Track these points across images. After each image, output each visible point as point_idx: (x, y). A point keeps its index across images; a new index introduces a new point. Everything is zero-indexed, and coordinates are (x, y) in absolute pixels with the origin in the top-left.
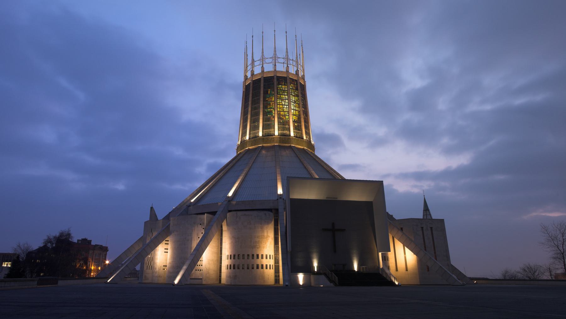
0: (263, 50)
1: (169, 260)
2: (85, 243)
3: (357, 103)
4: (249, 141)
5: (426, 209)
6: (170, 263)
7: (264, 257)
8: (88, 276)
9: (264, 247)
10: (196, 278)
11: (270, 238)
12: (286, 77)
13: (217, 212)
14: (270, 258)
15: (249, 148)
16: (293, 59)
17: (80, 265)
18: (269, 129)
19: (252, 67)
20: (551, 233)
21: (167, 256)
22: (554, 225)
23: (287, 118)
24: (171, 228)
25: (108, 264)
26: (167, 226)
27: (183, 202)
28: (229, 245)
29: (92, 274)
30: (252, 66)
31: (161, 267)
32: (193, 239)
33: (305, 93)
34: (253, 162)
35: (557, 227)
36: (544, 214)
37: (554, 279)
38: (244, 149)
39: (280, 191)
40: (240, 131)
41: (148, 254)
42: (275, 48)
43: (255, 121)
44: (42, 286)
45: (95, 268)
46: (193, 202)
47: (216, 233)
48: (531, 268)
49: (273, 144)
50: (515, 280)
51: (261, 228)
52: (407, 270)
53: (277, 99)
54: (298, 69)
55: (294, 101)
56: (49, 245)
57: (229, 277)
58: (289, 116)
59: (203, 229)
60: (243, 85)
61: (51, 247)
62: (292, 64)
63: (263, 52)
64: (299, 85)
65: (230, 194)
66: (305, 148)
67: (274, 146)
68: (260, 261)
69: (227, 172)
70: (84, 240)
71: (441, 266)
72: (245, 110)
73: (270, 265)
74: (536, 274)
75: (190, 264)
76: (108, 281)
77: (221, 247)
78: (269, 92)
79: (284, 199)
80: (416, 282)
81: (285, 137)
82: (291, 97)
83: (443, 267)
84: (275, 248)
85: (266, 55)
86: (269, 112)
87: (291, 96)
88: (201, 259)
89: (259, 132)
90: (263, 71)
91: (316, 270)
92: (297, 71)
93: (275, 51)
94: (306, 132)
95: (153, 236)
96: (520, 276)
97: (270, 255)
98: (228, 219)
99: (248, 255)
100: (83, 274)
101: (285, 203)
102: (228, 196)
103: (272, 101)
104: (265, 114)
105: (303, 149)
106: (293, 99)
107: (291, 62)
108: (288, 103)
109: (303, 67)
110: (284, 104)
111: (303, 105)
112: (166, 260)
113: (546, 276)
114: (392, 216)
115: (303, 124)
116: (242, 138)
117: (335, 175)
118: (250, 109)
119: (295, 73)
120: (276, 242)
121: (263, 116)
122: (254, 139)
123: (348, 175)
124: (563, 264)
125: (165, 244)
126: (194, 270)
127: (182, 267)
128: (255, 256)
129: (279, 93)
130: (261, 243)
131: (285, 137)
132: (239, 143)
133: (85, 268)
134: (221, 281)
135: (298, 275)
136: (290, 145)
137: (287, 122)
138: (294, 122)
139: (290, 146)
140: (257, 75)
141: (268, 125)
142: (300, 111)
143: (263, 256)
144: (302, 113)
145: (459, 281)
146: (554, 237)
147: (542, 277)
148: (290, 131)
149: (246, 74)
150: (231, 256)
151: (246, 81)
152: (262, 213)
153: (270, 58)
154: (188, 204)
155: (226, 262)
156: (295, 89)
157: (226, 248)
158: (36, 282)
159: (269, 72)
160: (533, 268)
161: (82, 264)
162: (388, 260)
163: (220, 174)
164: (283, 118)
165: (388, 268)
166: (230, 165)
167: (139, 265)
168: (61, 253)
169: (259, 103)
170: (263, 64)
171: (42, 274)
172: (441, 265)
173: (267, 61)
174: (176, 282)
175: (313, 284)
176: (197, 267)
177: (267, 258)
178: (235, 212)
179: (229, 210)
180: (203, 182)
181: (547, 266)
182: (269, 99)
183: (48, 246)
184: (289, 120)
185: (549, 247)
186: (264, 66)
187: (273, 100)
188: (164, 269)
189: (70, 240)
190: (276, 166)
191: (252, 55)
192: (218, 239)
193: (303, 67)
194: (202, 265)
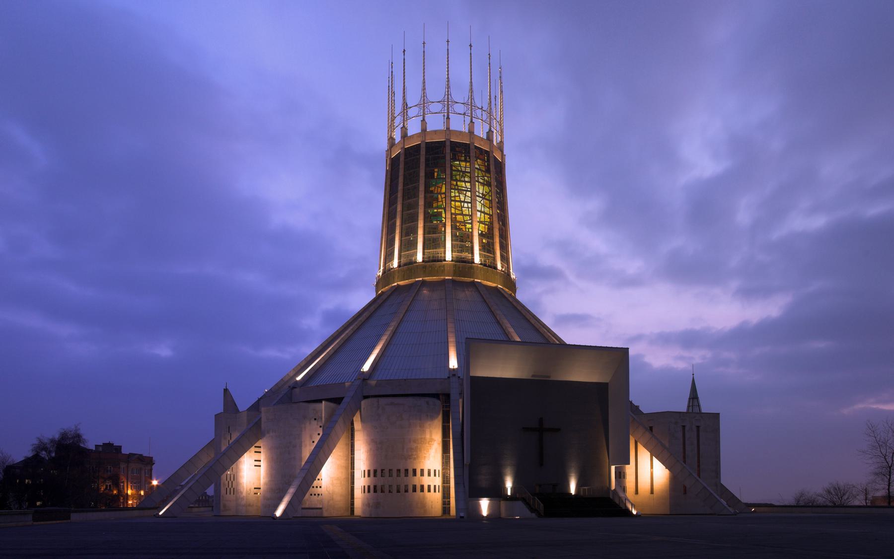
0: (424, 83)
1: (264, 479)
2: (110, 451)
3: (595, 204)
4: (399, 271)
5: (694, 397)
6: (265, 484)
7: (426, 473)
8: (123, 504)
9: (425, 457)
10: (313, 506)
11: (435, 442)
12: (469, 144)
13: (344, 398)
14: (435, 475)
15: (398, 283)
16: (482, 107)
17: (106, 488)
18: (436, 248)
19: (404, 120)
20: (879, 437)
21: (260, 472)
22: (887, 423)
23: (469, 229)
24: (263, 426)
25: (157, 485)
26: (256, 423)
27: (282, 379)
28: (366, 454)
29: (130, 502)
30: (404, 117)
31: (250, 490)
32: (303, 444)
33: (502, 179)
34: (407, 310)
35: (890, 427)
36: (875, 406)
37: (869, 504)
38: (390, 286)
39: (453, 363)
40: (381, 251)
41: (226, 469)
42: (448, 81)
43: (409, 232)
44: (42, 523)
45: (134, 492)
46: (299, 381)
47: (343, 433)
48: (839, 489)
49: (442, 277)
50: (812, 506)
51: (420, 426)
52: (652, 492)
53: (451, 189)
54: (492, 129)
55: (482, 194)
56: (43, 454)
57: (367, 505)
58: (471, 223)
59: (321, 427)
60: (387, 157)
61: (47, 459)
62: (480, 117)
63: (424, 89)
64: (492, 161)
65: (366, 367)
66: (499, 286)
67: (445, 280)
68: (419, 479)
69: (359, 328)
70: (108, 446)
71: (705, 487)
72: (391, 208)
73: (435, 486)
74: (845, 497)
75: (300, 485)
76: (161, 513)
77: (351, 457)
78: (436, 174)
79: (459, 377)
80: (664, 510)
81: (463, 264)
82: (477, 186)
83: (707, 487)
84: (443, 458)
85: (431, 96)
86: (435, 216)
87: (477, 183)
88: (318, 477)
89: (416, 253)
90: (424, 130)
91: (509, 493)
92: (490, 132)
93: (448, 87)
94: (502, 256)
95: (233, 439)
96: (821, 501)
97: (435, 471)
98: (362, 409)
99: (399, 471)
100: (115, 502)
101: (462, 385)
102: (362, 370)
103: (441, 194)
104: (428, 218)
105: (496, 288)
106: (481, 191)
107: (479, 112)
108: (471, 197)
109: (501, 125)
110: (463, 199)
111: (498, 203)
112: (259, 479)
113: (859, 501)
114: (637, 407)
115: (497, 240)
116: (385, 263)
117: (549, 336)
118: (398, 223)
119: (485, 137)
120: (445, 450)
121: (424, 223)
122: (408, 266)
123: (571, 336)
124: (887, 483)
125: (255, 452)
126: (307, 495)
127: (288, 490)
128: (411, 472)
129: (453, 178)
130: (421, 451)
131: (463, 264)
132: (381, 274)
133: (115, 492)
134: (354, 511)
135: (480, 501)
136: (472, 279)
137: (468, 235)
138: (481, 235)
139: (473, 282)
140: (412, 136)
141: (434, 241)
142: (492, 215)
143: (423, 471)
144: (495, 218)
145: (728, 507)
146: (882, 442)
147: (853, 502)
148: (472, 253)
149: (391, 134)
150: (369, 471)
151: (392, 148)
152: (422, 401)
153: (439, 102)
154: (291, 383)
155: (360, 482)
156: (484, 170)
157: (360, 460)
158: (30, 517)
159: (435, 132)
160: (842, 488)
161: (110, 486)
162: (624, 478)
163: (347, 332)
164: (461, 227)
165: (624, 489)
166: (365, 315)
167: (213, 485)
168: (68, 468)
169: (416, 196)
170: (424, 114)
171: (38, 503)
172: (705, 485)
174: (278, 513)
175: (503, 515)
176: (311, 490)
177: (429, 475)
178: (375, 399)
179: (365, 395)
180: (315, 346)
181: (863, 486)
182: (436, 190)
183: (42, 456)
184: (472, 232)
185: (871, 458)
186: (426, 119)
187: (443, 190)
188: (257, 494)
189: (82, 445)
190: (447, 319)
191: (404, 93)
192: (347, 444)
193: (501, 125)
194: (320, 487)
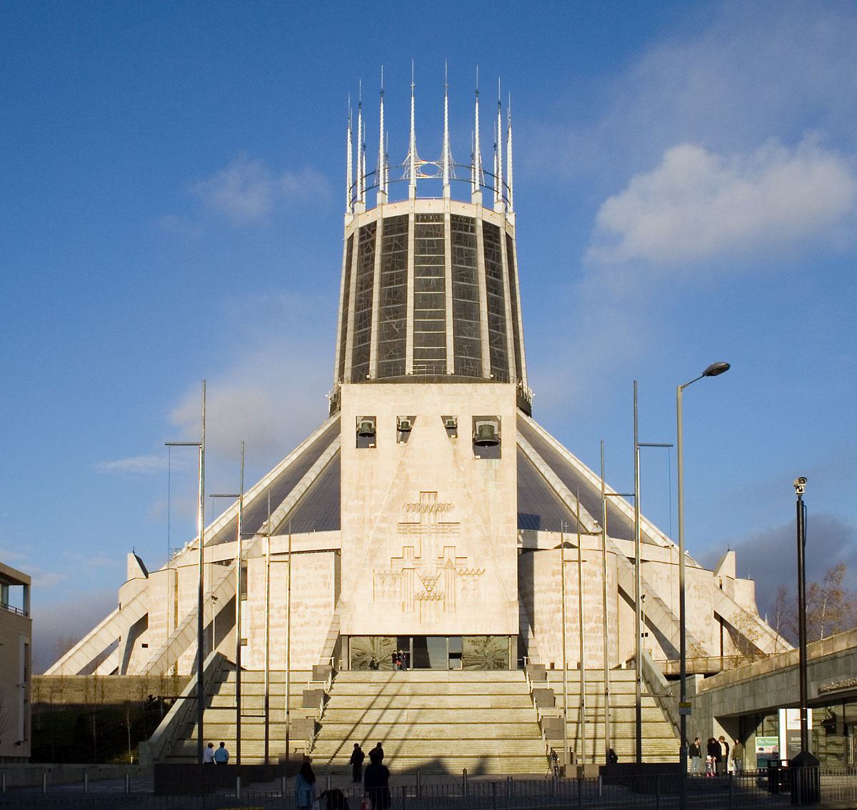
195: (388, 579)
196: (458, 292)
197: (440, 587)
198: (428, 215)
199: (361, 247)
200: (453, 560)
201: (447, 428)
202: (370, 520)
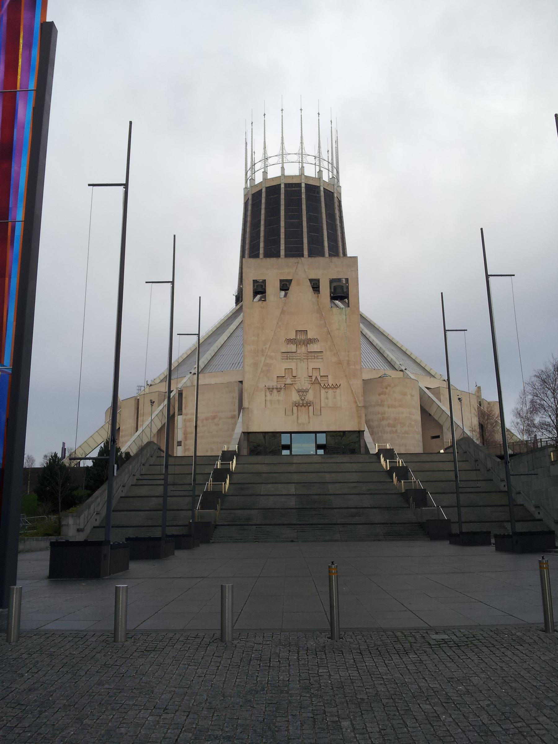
85: (287, 149)
90: (283, 174)
159: (292, 177)
170: (283, 163)
173: (290, 158)
195: (275, 391)
196: (310, 229)
197: (310, 396)
198: (292, 184)
199: (253, 205)
200: (319, 378)
201: (312, 288)
202: (262, 351)
